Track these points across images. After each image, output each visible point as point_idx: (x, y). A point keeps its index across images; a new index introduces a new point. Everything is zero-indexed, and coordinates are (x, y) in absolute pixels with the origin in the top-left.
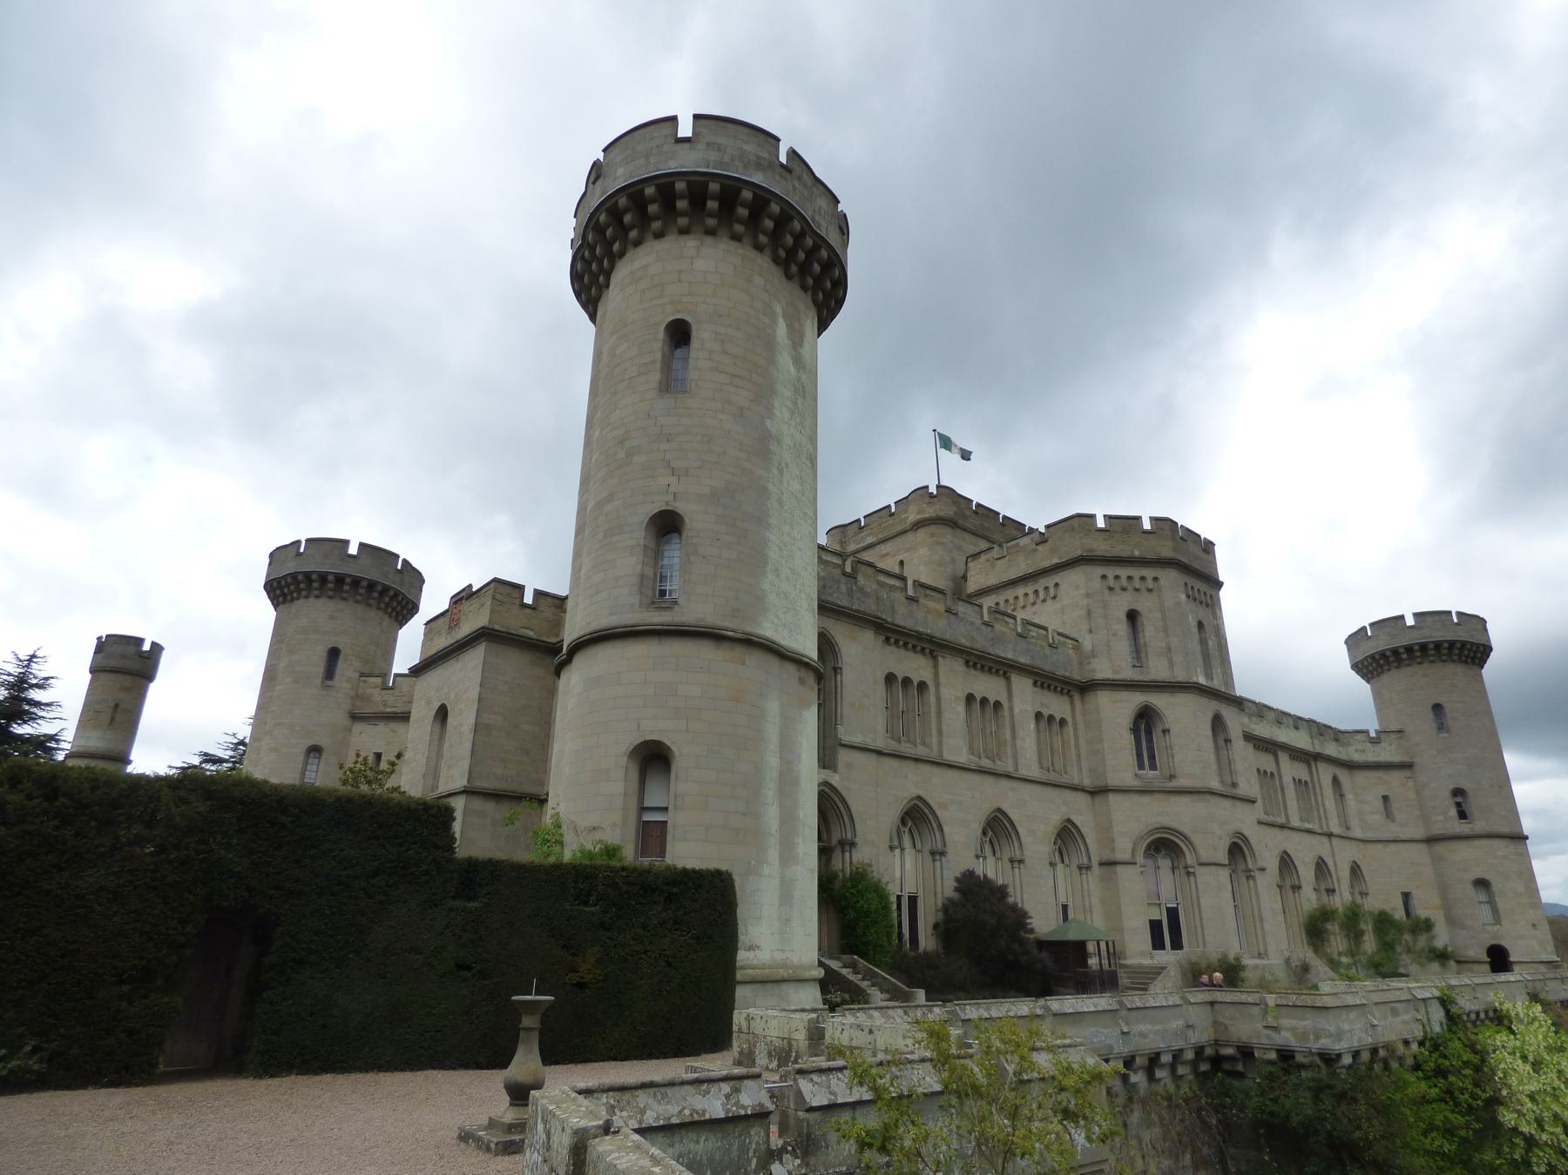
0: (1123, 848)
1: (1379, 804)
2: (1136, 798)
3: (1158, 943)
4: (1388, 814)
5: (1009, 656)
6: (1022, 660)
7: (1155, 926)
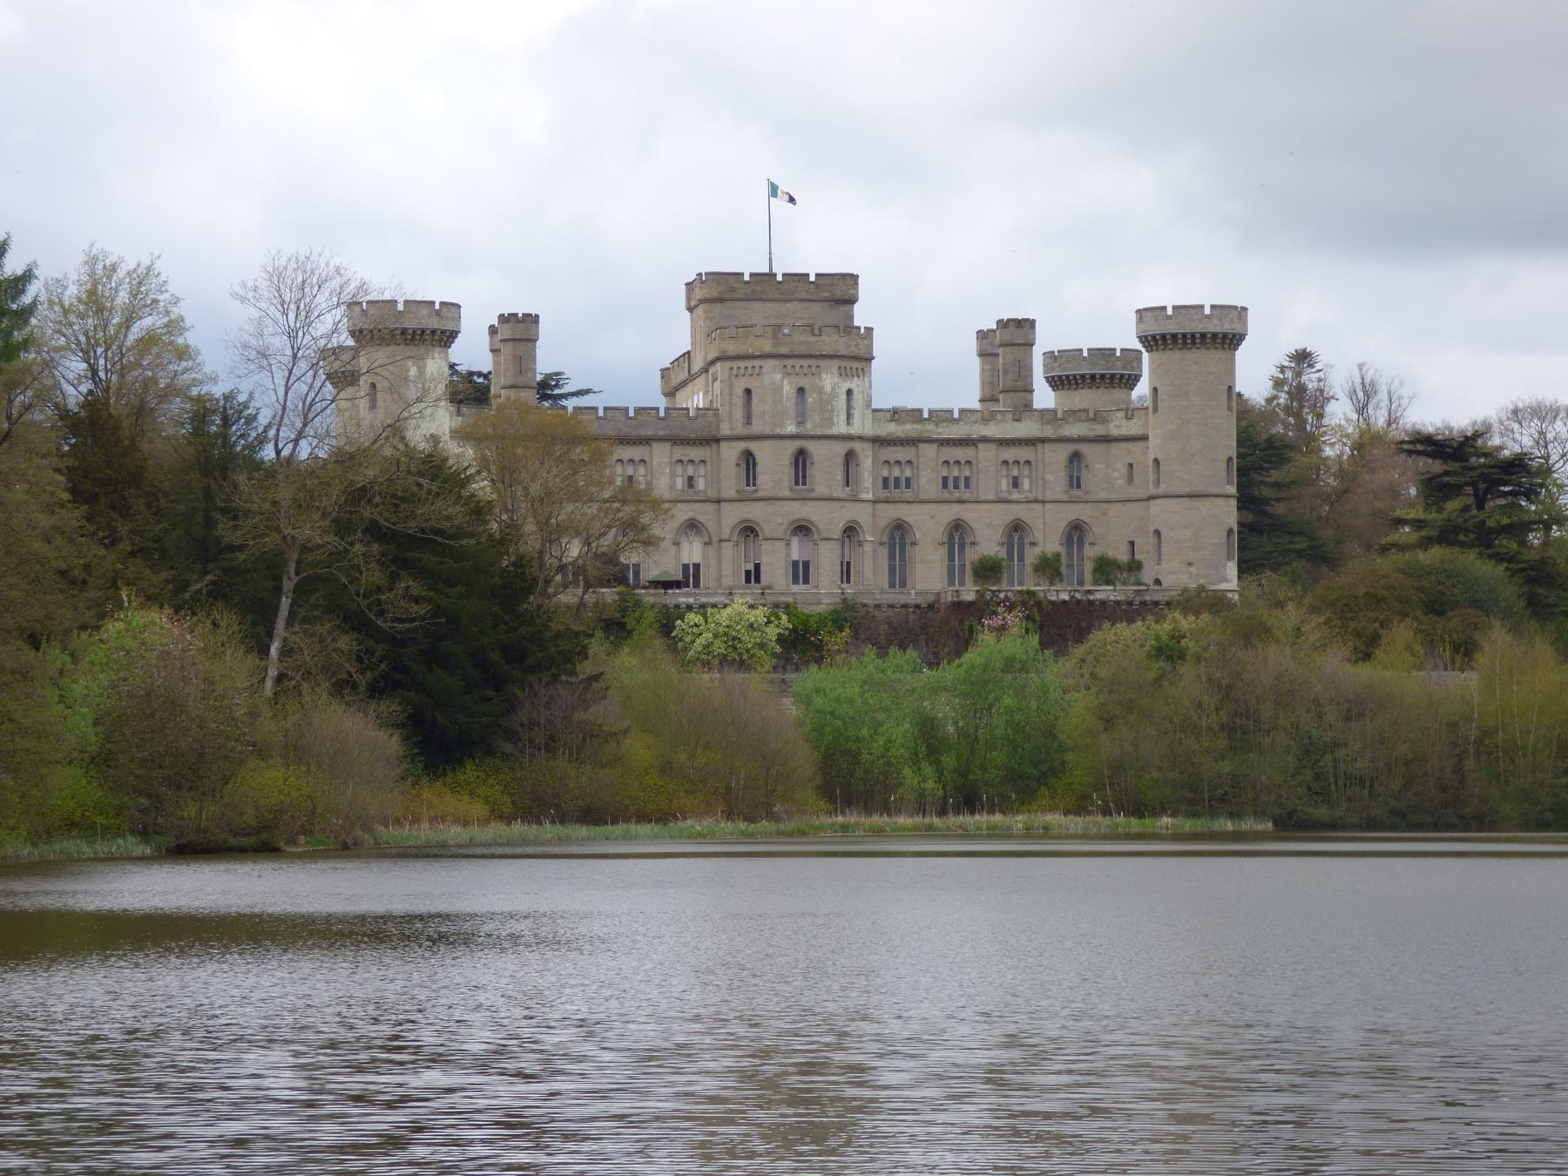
0: (726, 533)
1: (1124, 470)
2: (736, 505)
3: (748, 580)
4: (1130, 479)
5: (650, 433)
6: (661, 433)
7: (748, 573)
